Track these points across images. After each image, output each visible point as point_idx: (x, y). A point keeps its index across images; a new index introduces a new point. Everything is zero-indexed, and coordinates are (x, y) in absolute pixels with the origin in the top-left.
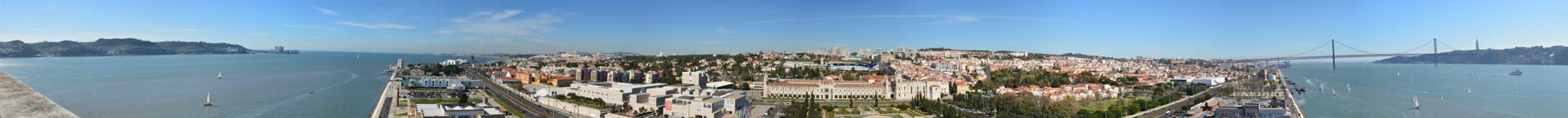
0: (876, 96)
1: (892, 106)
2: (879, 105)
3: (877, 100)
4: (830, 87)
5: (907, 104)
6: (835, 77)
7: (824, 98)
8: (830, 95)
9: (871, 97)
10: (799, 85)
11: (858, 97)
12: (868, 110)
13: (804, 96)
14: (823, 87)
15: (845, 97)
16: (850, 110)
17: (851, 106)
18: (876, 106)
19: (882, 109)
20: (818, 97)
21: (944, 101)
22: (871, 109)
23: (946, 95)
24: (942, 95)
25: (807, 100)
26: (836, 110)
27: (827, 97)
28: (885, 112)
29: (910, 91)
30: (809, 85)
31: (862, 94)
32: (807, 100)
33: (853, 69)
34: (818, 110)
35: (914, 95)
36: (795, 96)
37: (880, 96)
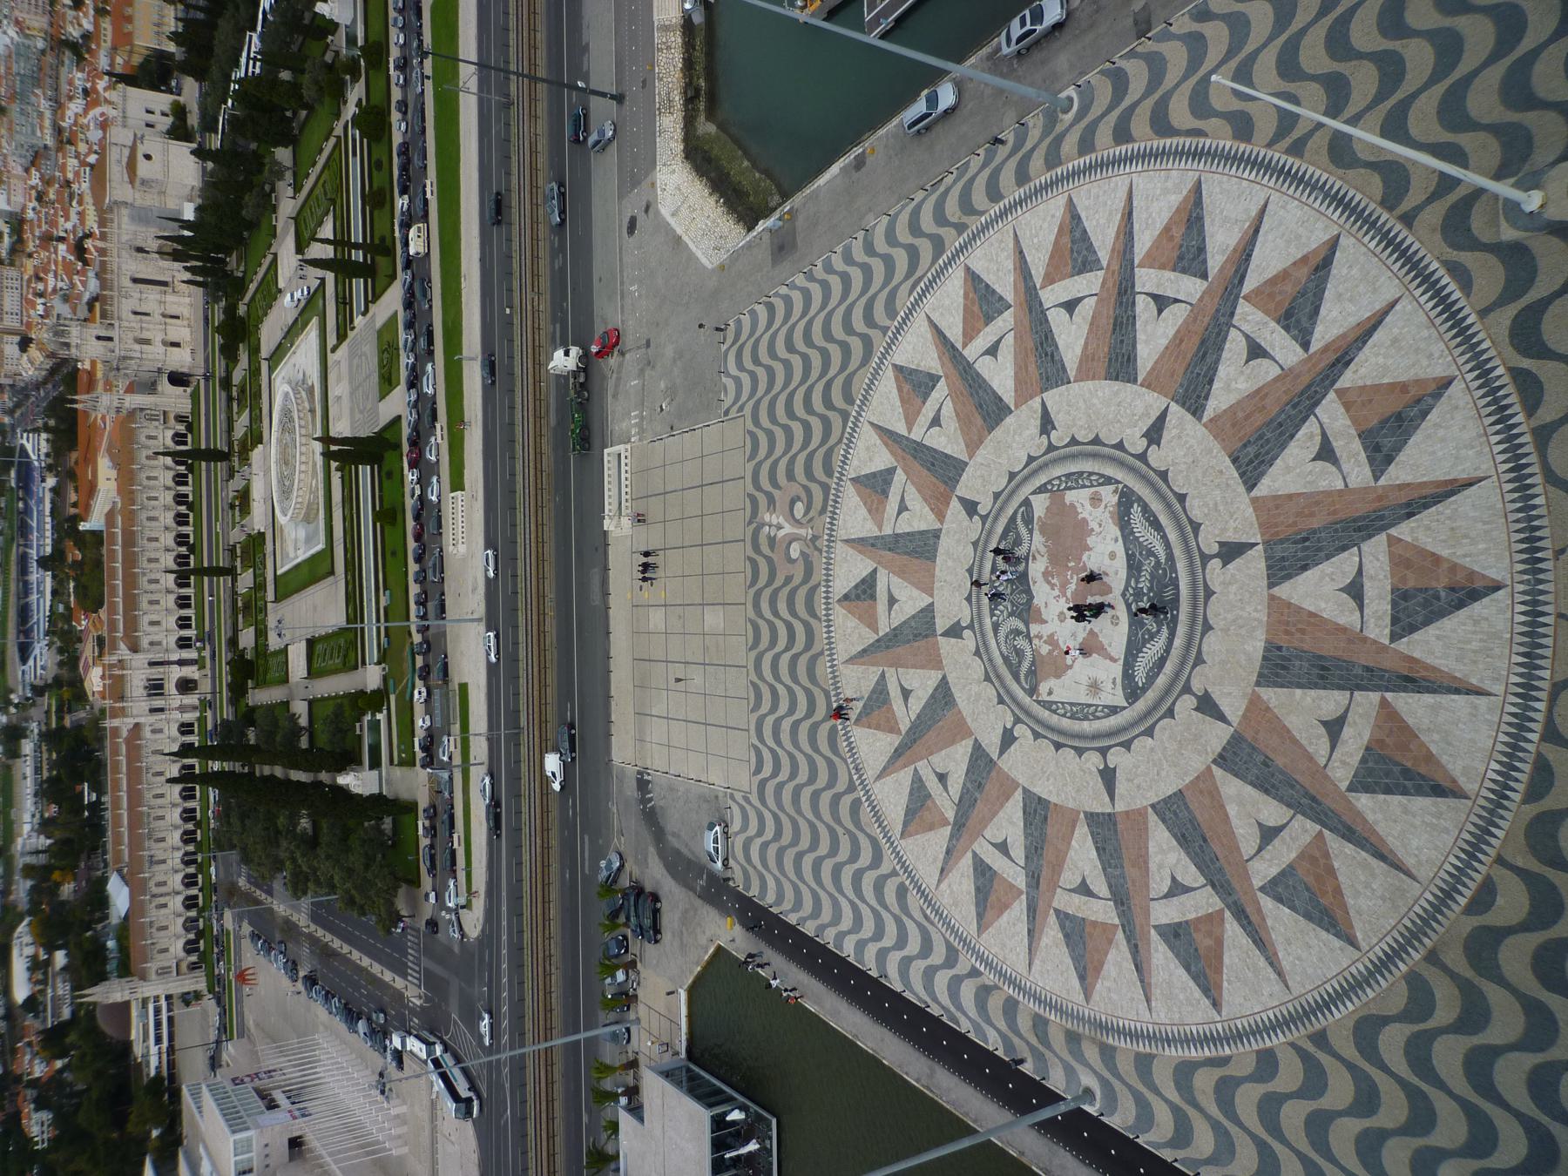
0: (178, 457)
1: (226, 383)
2: (221, 445)
3: (197, 454)
4: (137, 679)
5: (218, 317)
6: (88, 650)
7: (192, 699)
8: (176, 673)
9: (180, 480)
10: (136, 821)
11: (181, 539)
12: (244, 497)
13: (188, 795)
14: (138, 705)
15: (183, 602)
16: (246, 580)
17: (230, 572)
18: (223, 456)
19: (240, 430)
20: (186, 728)
21: (209, 125)
22: (237, 484)
23: (179, 112)
24: (179, 132)
25: (208, 779)
26: (247, 638)
27: (186, 686)
28: (256, 419)
29: (153, 293)
30: (135, 775)
31: (168, 518)
32: (208, 779)
33: (44, 563)
34: (252, 723)
35: (177, 272)
36: (188, 838)
37: (179, 438)
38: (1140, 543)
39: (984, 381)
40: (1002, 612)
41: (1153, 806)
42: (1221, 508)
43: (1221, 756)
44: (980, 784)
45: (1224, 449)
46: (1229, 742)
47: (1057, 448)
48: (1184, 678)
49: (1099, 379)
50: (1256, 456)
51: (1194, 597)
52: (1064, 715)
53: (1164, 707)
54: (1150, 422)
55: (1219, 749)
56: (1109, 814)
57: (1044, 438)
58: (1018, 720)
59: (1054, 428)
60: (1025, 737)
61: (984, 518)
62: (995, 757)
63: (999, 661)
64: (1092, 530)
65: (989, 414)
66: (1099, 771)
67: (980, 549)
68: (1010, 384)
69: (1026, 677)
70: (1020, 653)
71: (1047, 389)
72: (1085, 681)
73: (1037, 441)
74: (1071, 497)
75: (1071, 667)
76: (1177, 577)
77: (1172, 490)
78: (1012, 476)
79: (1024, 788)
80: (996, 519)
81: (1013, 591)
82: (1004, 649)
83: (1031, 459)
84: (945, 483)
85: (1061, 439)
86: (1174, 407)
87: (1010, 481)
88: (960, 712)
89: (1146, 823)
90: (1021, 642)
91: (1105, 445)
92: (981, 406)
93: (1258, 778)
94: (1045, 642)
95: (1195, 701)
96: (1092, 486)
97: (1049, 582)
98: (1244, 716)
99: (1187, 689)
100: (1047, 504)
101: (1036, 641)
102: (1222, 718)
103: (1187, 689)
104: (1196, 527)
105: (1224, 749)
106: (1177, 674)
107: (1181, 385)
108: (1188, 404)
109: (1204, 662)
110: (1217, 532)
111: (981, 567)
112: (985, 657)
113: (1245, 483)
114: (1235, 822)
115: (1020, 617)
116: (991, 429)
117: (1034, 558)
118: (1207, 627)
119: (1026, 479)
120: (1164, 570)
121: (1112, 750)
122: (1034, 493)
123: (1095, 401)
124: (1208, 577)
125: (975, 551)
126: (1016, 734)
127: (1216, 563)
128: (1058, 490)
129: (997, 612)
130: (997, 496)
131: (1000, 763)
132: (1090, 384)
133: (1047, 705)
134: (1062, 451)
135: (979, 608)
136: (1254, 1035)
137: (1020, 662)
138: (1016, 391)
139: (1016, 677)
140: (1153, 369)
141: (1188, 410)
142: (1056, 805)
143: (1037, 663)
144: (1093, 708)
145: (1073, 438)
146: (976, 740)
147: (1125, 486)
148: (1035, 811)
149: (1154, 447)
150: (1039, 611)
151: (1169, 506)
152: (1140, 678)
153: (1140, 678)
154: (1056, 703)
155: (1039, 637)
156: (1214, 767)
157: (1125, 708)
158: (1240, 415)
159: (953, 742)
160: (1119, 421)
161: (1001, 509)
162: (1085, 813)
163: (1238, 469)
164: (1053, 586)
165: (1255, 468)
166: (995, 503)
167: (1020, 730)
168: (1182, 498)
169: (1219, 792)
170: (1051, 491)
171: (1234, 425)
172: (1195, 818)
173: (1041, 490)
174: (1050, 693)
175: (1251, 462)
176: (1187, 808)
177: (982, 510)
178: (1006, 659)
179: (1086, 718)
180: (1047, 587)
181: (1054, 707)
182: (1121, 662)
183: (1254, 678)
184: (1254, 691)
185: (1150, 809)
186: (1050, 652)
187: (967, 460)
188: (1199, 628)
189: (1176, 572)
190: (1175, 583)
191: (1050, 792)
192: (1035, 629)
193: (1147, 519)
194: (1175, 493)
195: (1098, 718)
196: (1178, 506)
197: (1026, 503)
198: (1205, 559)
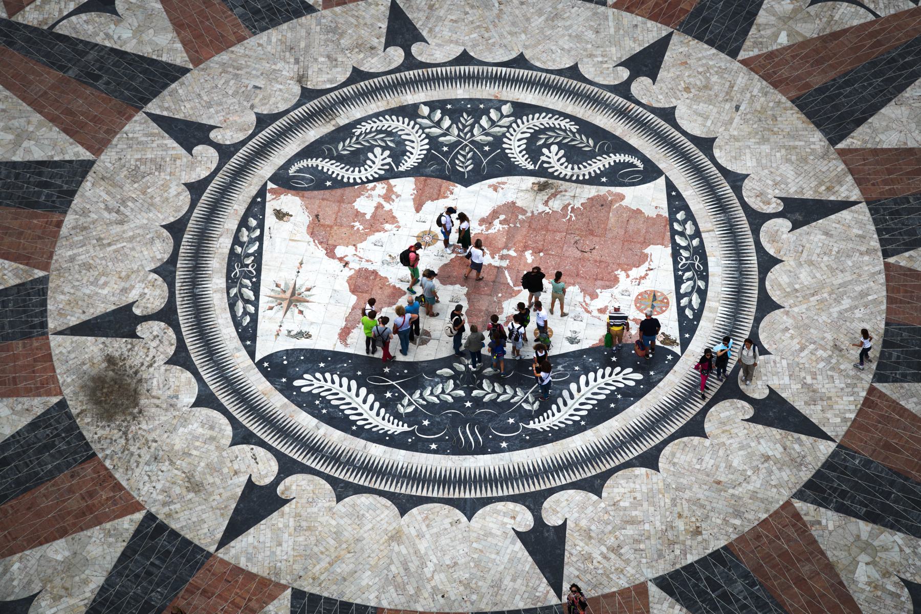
38: (566, 384)
39: (902, 88)
40: (438, 124)
41: (62, 404)
42: (630, 531)
43: (162, 528)
44: (97, 78)
45: (741, 539)
46: (188, 543)
47: (756, 232)
48: (309, 462)
49: (889, 311)
50: (724, 596)
51: (463, 481)
52: (237, 241)
53: (256, 428)
54: (799, 405)
55: (174, 525)
56: (44, 325)
57: (775, 206)
58: (226, 152)
59: (796, 226)
60: (191, 167)
61: (623, 89)
62: (153, 107)
63: (344, 117)
64: (594, 296)
65: (832, 98)
66: (129, 306)
67: (563, 80)
68: (890, 140)
69: (314, 170)
70: (356, 159)
71: (873, 211)
72: (303, 282)
73: (771, 193)
74: (660, 255)
75: (331, 253)
76: (499, 450)
77: (665, 443)
78: (706, 144)
79: (91, 163)
80: (622, 113)
81: (479, 145)
82: (367, 126)
83: (736, 180)
84: (698, 11)
85: (773, 240)
86: (825, 449)
87: (694, 139)
88: (241, 39)
89: (29, 392)
90: (379, 160)
91: (758, 320)
92: (848, 83)
93: (119, 595)
94: (379, 207)
95: (267, 481)
96: (679, 297)
97: (495, 214)
98: (237, 570)
99: (288, 467)
100: (651, 213)
101: (381, 188)
102: (235, 529)
103: (288, 467)
104: (594, 486)
105: (174, 534)
106: (314, 449)
107: (867, 463)
108: (832, 474)
109: (339, 499)
110: (584, 523)
111: (530, 84)
112: (348, 90)
113: (675, 575)
114: (33, 555)
115: (428, 158)
116: (801, 104)
117: (542, 187)
118: (404, 504)
119: (697, 171)
120: (514, 427)
121: (171, 332)
122: (670, 186)
123: (846, 303)
124: (500, 506)
125: (560, 72)
126: (198, 149)
127: (525, 520)
128: (674, 232)
129: (438, 115)
130: (668, 115)
131: (140, 117)
132: (878, 291)
133: (256, 207)
134: (751, 240)
135: (448, 79)
136: (594, 459)
137: (340, 159)
138: (875, 152)
139: (309, 151)
140: (903, 411)
141: (818, 474)
142: (59, 224)
143: (339, 192)
144: (249, 294)
145: (776, 261)
146: (184, 71)
147: (676, 358)
148: (46, 185)
149: (749, 411)
150: (439, 195)
151: (635, 436)
152: (308, 383)
153: (308, 383)
154: (261, 225)
155: (388, 197)
156: (139, 516)
157: (252, 354)
158: (805, 570)
159: (178, 26)
160: (802, 349)
161: (642, 125)
162: (44, 280)
163: (702, 562)
164: (487, 221)
165: (702, 594)
166: (653, 110)
167: (207, 157)
168: (650, 460)
169: (89, 526)
170: (672, 219)
171: (784, 555)
172: (40, 482)
173: (676, 200)
174: (280, 215)
175: (715, 586)
176: (59, 469)
177: (641, 87)
178: (345, 131)
179: (231, 281)
180: (485, 212)
181: (253, 222)
182: (340, 348)
183: (307, 589)
184: (285, 587)
185: (55, 400)
186: (358, 215)
187: (743, 55)
188: (405, 489)
189: (510, 449)
190: (489, 447)
191: (85, 213)
192: (405, 187)
193: (611, 397)
194: (659, 448)
195: (232, 306)
196: (635, 452)
197: (651, 172)
198: (534, 502)
